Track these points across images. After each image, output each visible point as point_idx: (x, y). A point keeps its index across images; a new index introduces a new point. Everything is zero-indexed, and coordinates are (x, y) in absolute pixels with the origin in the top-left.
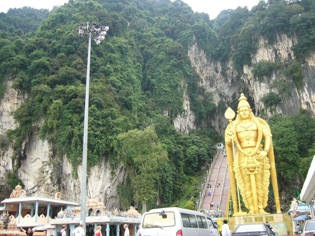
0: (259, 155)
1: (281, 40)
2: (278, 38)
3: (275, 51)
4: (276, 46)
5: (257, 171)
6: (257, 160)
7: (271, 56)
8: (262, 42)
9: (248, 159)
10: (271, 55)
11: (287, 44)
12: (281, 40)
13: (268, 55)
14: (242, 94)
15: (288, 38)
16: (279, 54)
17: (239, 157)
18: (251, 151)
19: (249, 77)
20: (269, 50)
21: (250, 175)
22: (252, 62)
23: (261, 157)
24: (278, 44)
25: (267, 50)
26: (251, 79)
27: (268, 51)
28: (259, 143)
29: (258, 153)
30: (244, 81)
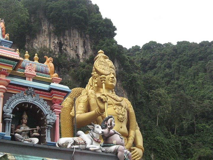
0: (134, 151)
1: (70, 36)
2: (67, 32)
3: (60, 45)
4: (62, 39)
8: (45, 27)
11: (77, 42)
12: (70, 36)
13: (50, 45)
14: (100, 51)
15: (79, 36)
16: (65, 50)
20: (52, 41)
22: (26, 46)
23: (136, 156)
24: (65, 38)
29: (132, 148)
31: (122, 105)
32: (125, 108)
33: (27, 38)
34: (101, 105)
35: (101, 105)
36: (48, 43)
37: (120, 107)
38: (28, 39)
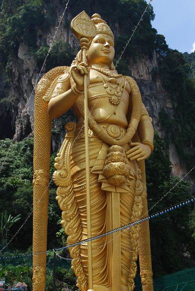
5: (128, 189)
6: (129, 159)
7: (74, 43)
9: (108, 152)
10: (73, 41)
13: (68, 40)
17: (74, 147)
18: (116, 135)
19: (25, 67)
21: (104, 194)
25: (68, 33)
26: (28, 70)
27: (68, 35)
28: (134, 123)
29: (132, 144)
30: (13, 71)
31: (118, 82)
32: (123, 87)
33: (39, 32)
34: (79, 80)
35: (79, 80)
36: (66, 38)
37: (114, 86)
38: (40, 35)
